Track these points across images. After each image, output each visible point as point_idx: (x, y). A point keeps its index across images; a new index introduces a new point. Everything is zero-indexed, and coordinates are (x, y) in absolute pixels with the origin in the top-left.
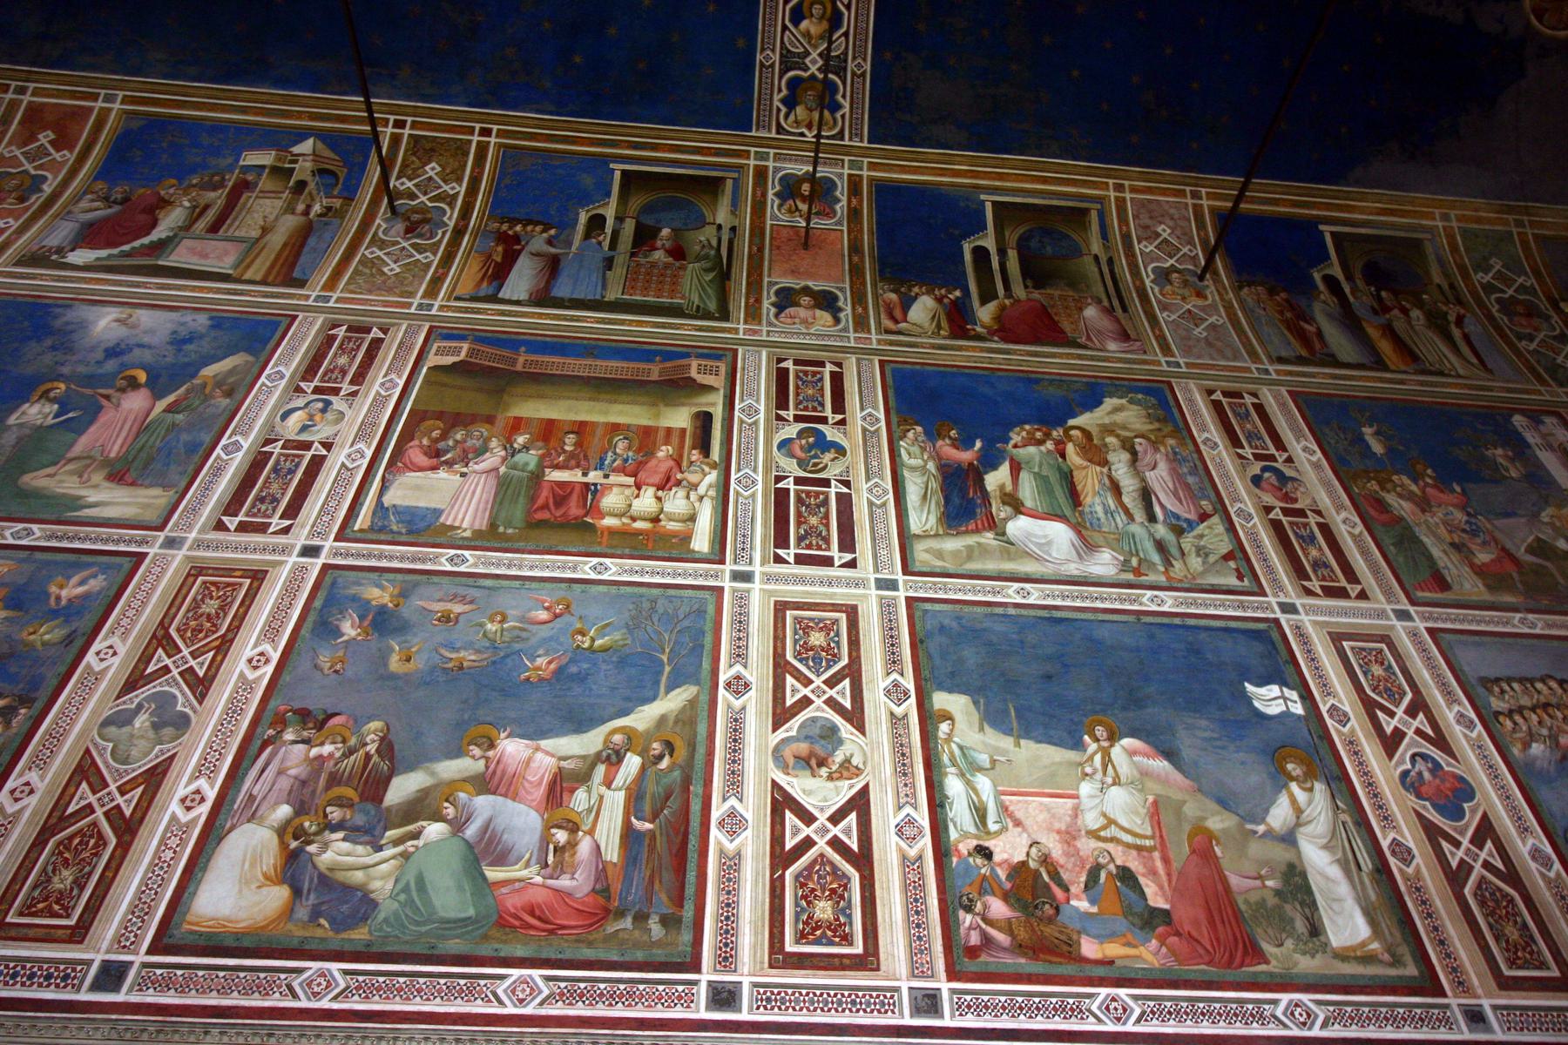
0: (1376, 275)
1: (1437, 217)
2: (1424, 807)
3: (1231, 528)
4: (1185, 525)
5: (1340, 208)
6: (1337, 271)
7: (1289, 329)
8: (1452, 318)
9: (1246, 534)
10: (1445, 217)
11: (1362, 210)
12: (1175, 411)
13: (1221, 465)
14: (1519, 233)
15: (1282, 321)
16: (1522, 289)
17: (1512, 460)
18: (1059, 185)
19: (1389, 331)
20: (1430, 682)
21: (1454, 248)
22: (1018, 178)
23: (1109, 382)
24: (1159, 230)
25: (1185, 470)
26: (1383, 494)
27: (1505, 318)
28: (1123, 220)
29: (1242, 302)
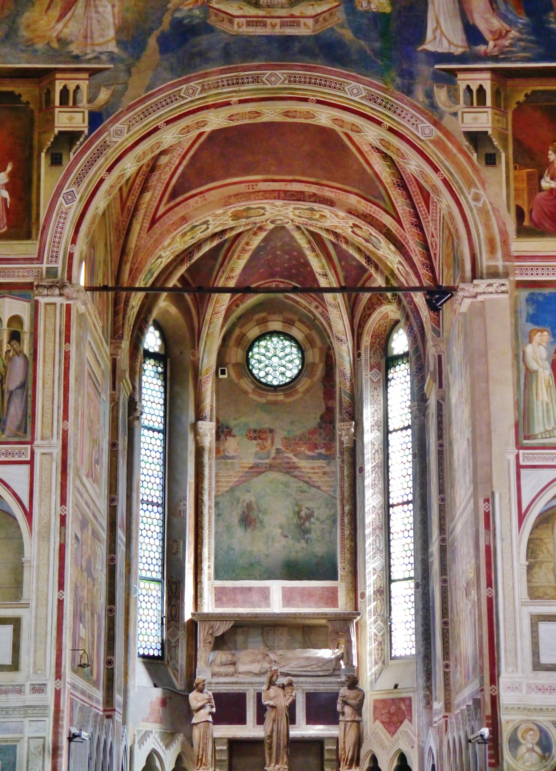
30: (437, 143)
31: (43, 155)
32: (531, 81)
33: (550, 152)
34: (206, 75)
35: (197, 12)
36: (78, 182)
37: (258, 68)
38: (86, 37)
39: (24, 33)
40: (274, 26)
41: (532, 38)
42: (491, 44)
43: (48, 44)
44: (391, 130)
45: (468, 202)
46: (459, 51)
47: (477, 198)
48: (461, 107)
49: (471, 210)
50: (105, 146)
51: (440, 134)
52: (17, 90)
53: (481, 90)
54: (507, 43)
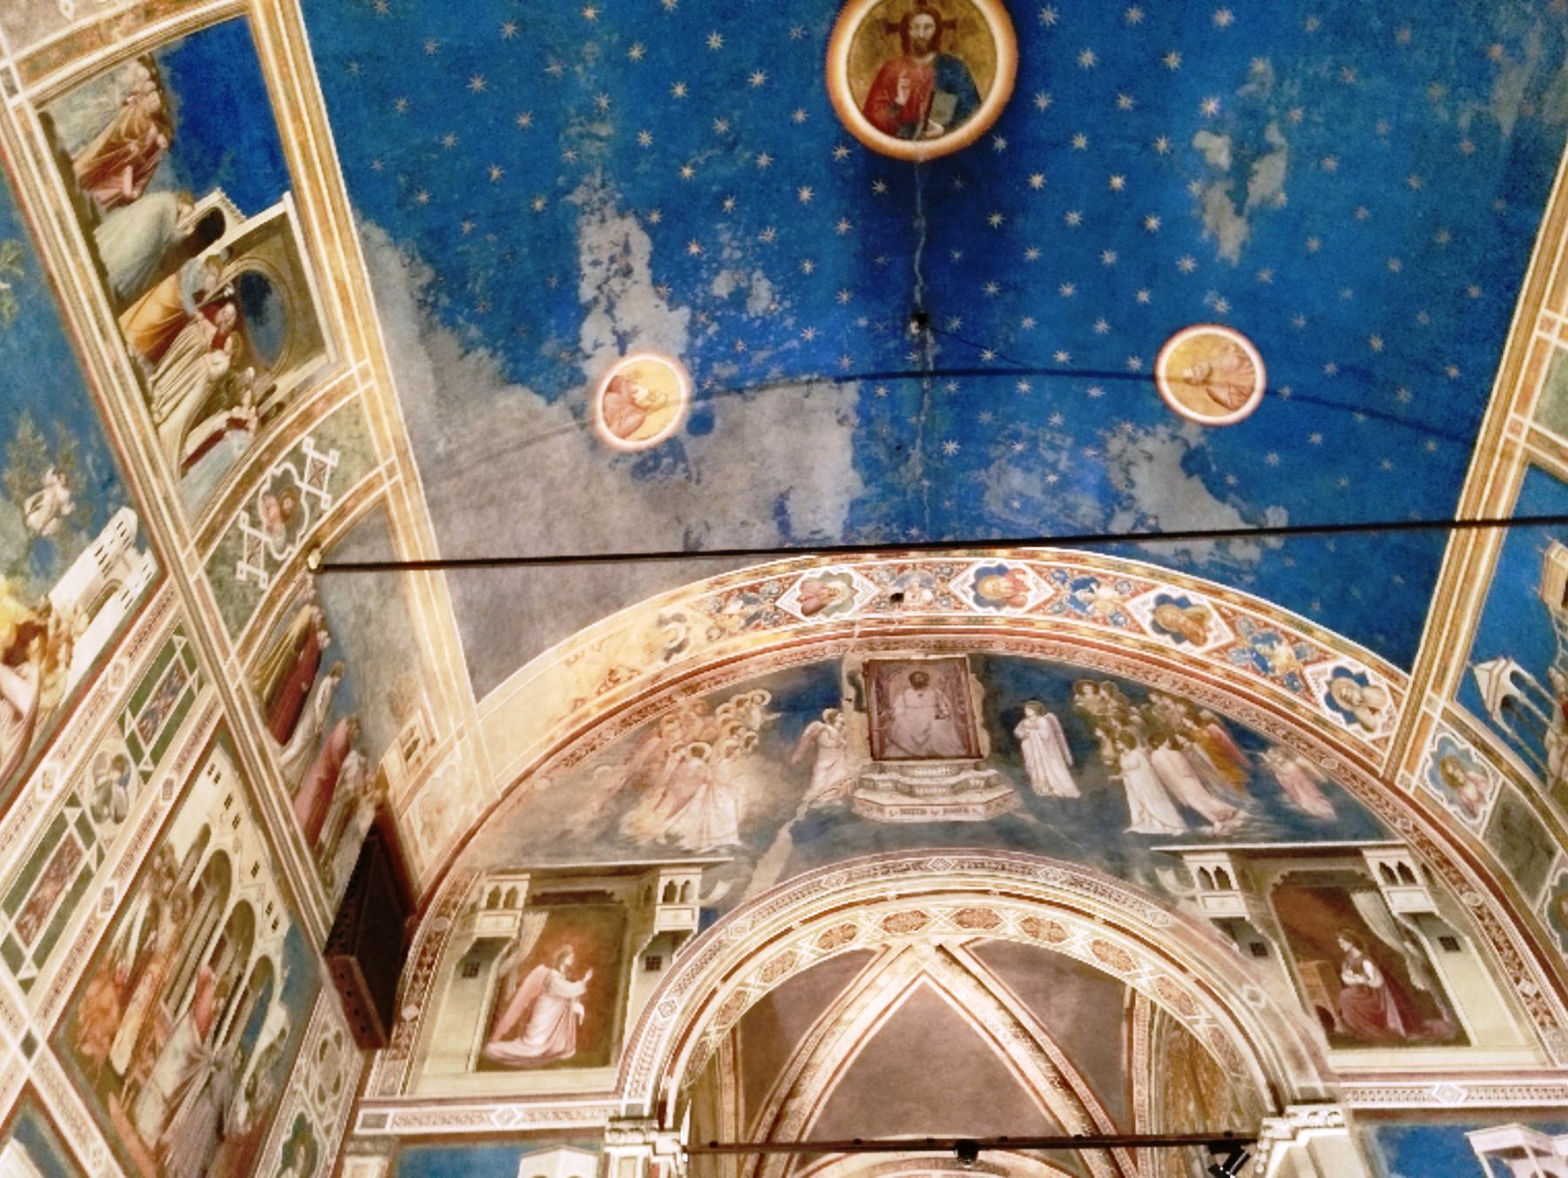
0: (252, 291)
1: (361, 364)
5: (324, 220)
6: (237, 228)
7: (109, 146)
8: (237, 413)
10: (365, 375)
11: (332, 255)
14: (379, 475)
15: (117, 133)
16: (315, 501)
17: (57, 514)
19: (175, 325)
21: (329, 398)
27: (267, 487)
29: (116, 61)
30: (1175, 930)
31: (636, 959)
32: (1284, 862)
33: (1341, 940)
34: (855, 863)
35: (839, 803)
36: (681, 989)
37: (919, 855)
38: (701, 832)
39: (626, 831)
40: (935, 813)
41: (1269, 818)
42: (1218, 825)
43: (654, 841)
44: (1107, 923)
45: (1243, 1003)
46: (1178, 832)
47: (1254, 997)
48: (1198, 889)
49: (1252, 1013)
50: (720, 945)
51: (1178, 921)
52: (609, 890)
53: (1219, 872)
54: (1238, 823)
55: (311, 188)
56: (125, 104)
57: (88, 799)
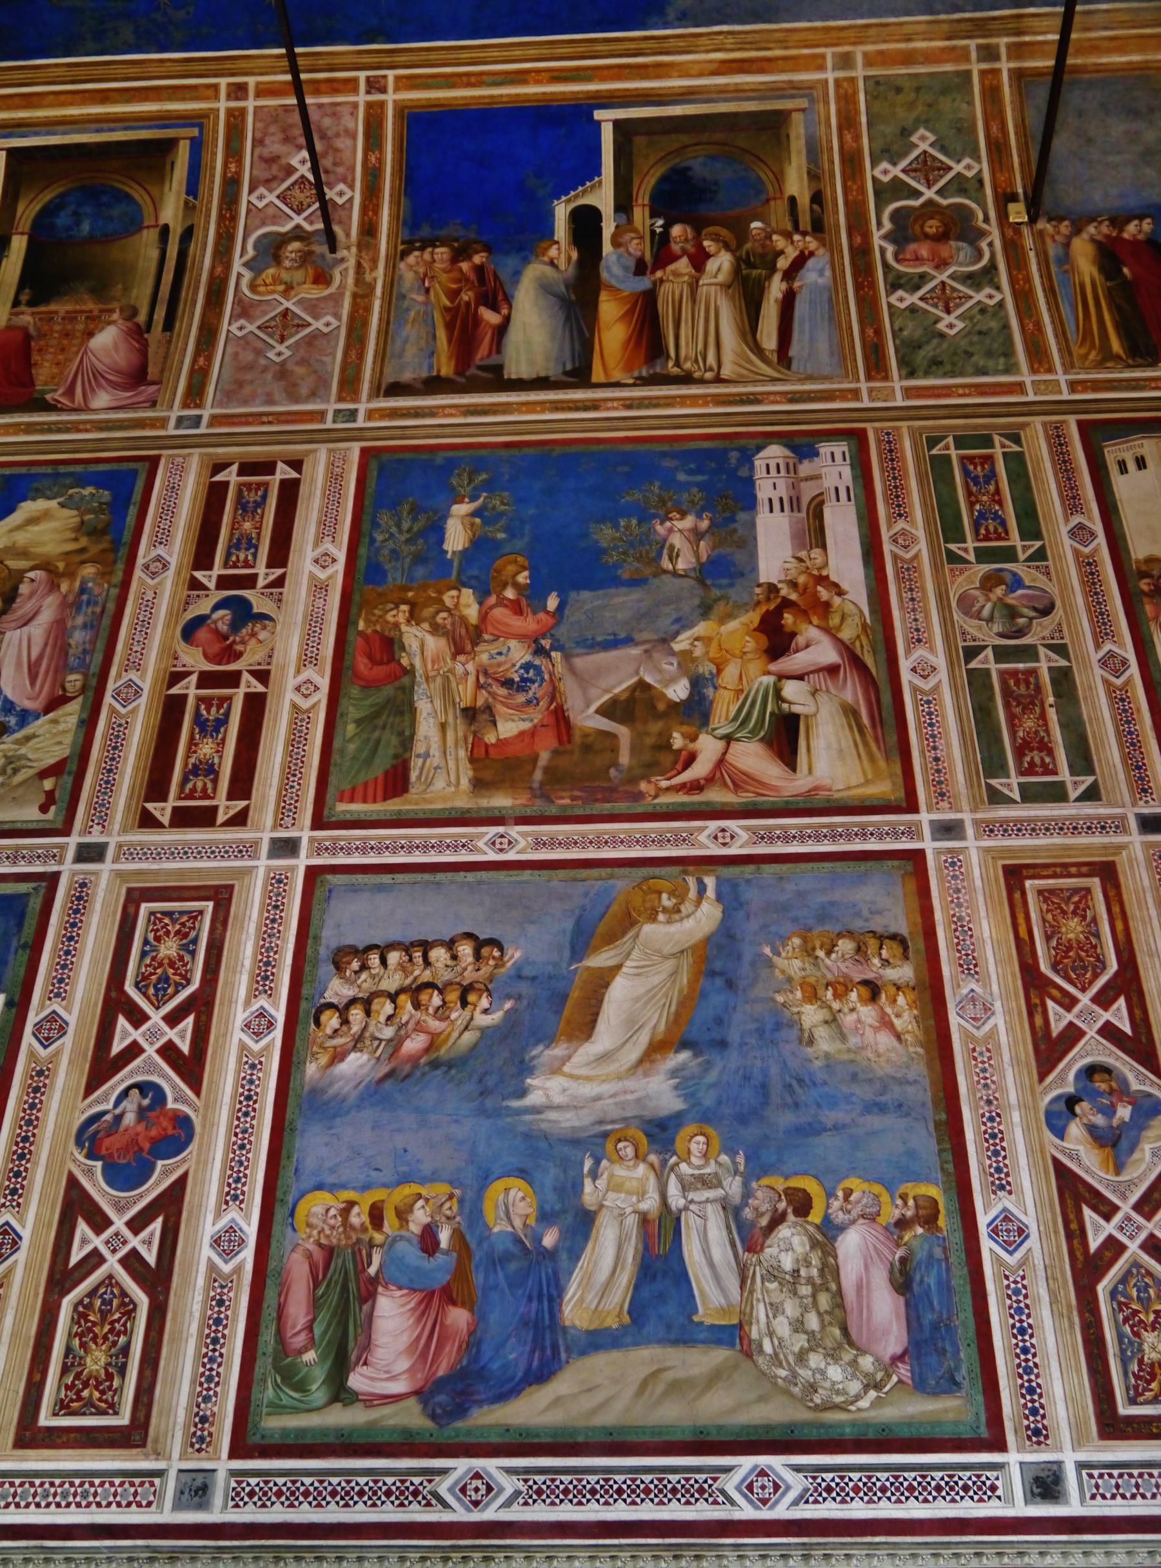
2: (89, 1172)
3: (89, 724)
4: (13, 721)
5: (642, 71)
9: (109, 725)
10: (845, 61)
11: (683, 71)
12: (133, 511)
13: (149, 607)
16: (960, 185)
18: (128, 101)
20: (248, 963)
21: (848, 121)
22: (60, 99)
23: (49, 470)
24: (295, 162)
25: (80, 620)
26: (404, 628)
28: (234, 152)
29: (392, 283)
55: (603, 79)
56: (427, 291)
57: (989, 635)
